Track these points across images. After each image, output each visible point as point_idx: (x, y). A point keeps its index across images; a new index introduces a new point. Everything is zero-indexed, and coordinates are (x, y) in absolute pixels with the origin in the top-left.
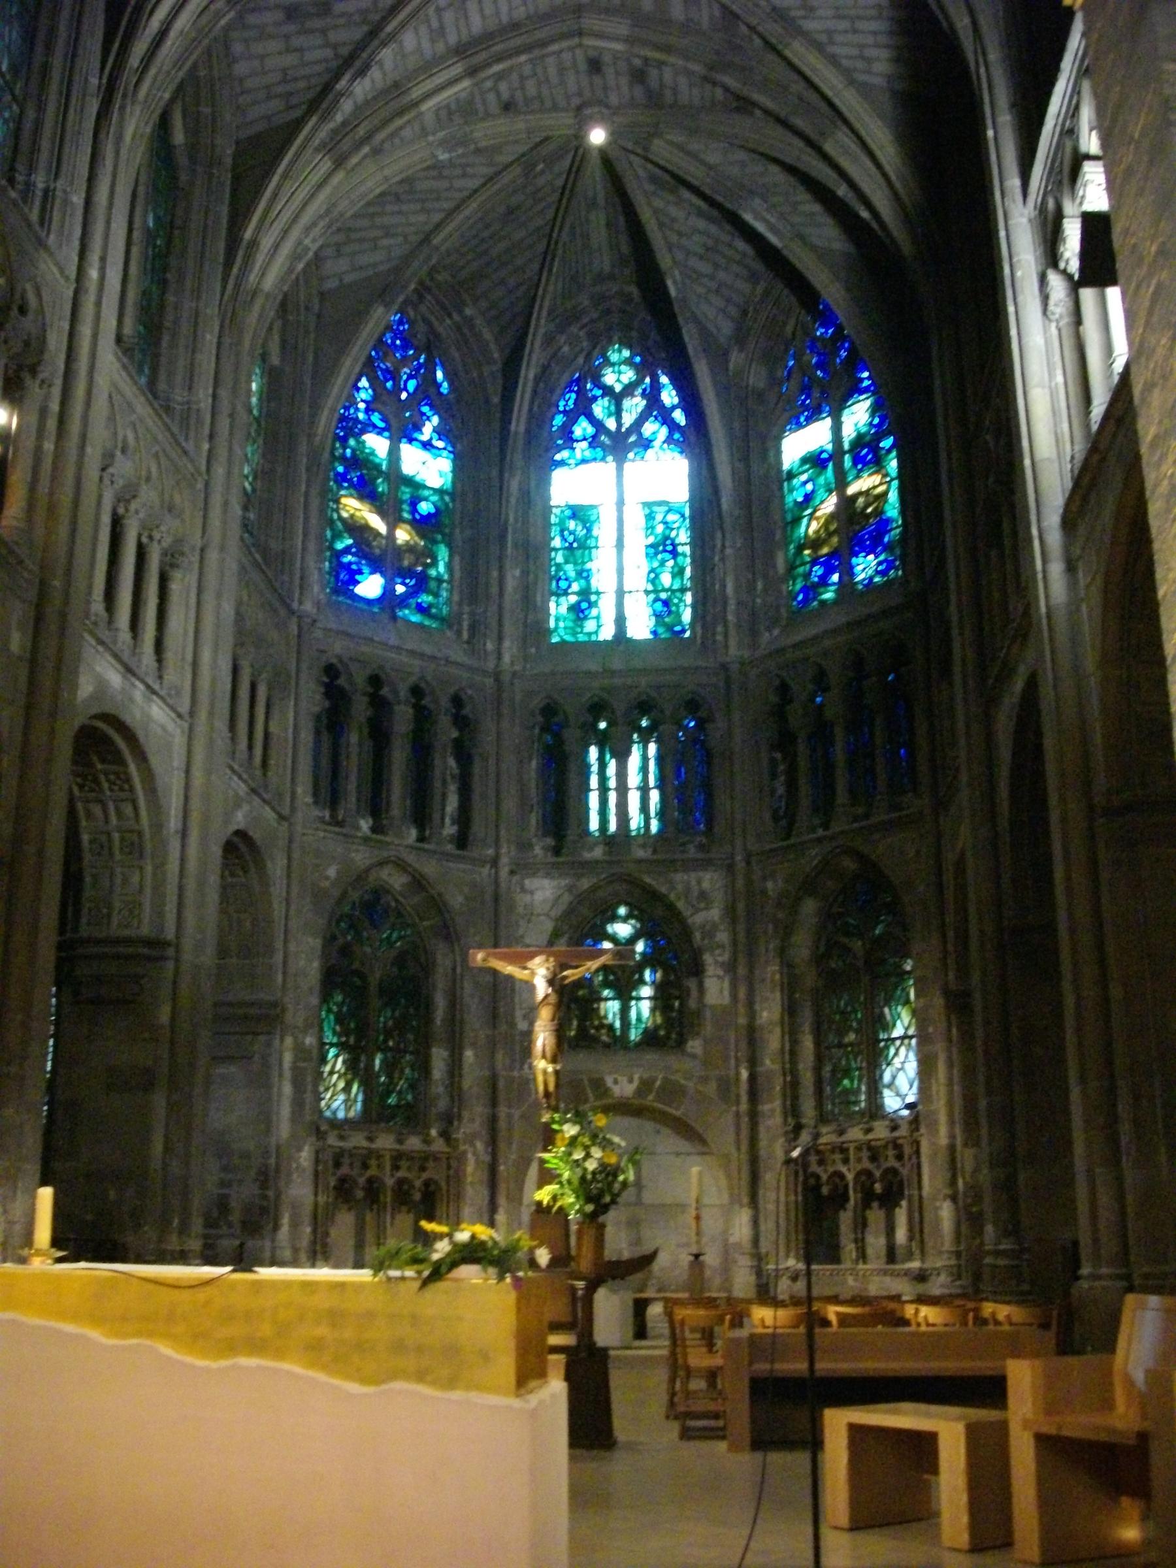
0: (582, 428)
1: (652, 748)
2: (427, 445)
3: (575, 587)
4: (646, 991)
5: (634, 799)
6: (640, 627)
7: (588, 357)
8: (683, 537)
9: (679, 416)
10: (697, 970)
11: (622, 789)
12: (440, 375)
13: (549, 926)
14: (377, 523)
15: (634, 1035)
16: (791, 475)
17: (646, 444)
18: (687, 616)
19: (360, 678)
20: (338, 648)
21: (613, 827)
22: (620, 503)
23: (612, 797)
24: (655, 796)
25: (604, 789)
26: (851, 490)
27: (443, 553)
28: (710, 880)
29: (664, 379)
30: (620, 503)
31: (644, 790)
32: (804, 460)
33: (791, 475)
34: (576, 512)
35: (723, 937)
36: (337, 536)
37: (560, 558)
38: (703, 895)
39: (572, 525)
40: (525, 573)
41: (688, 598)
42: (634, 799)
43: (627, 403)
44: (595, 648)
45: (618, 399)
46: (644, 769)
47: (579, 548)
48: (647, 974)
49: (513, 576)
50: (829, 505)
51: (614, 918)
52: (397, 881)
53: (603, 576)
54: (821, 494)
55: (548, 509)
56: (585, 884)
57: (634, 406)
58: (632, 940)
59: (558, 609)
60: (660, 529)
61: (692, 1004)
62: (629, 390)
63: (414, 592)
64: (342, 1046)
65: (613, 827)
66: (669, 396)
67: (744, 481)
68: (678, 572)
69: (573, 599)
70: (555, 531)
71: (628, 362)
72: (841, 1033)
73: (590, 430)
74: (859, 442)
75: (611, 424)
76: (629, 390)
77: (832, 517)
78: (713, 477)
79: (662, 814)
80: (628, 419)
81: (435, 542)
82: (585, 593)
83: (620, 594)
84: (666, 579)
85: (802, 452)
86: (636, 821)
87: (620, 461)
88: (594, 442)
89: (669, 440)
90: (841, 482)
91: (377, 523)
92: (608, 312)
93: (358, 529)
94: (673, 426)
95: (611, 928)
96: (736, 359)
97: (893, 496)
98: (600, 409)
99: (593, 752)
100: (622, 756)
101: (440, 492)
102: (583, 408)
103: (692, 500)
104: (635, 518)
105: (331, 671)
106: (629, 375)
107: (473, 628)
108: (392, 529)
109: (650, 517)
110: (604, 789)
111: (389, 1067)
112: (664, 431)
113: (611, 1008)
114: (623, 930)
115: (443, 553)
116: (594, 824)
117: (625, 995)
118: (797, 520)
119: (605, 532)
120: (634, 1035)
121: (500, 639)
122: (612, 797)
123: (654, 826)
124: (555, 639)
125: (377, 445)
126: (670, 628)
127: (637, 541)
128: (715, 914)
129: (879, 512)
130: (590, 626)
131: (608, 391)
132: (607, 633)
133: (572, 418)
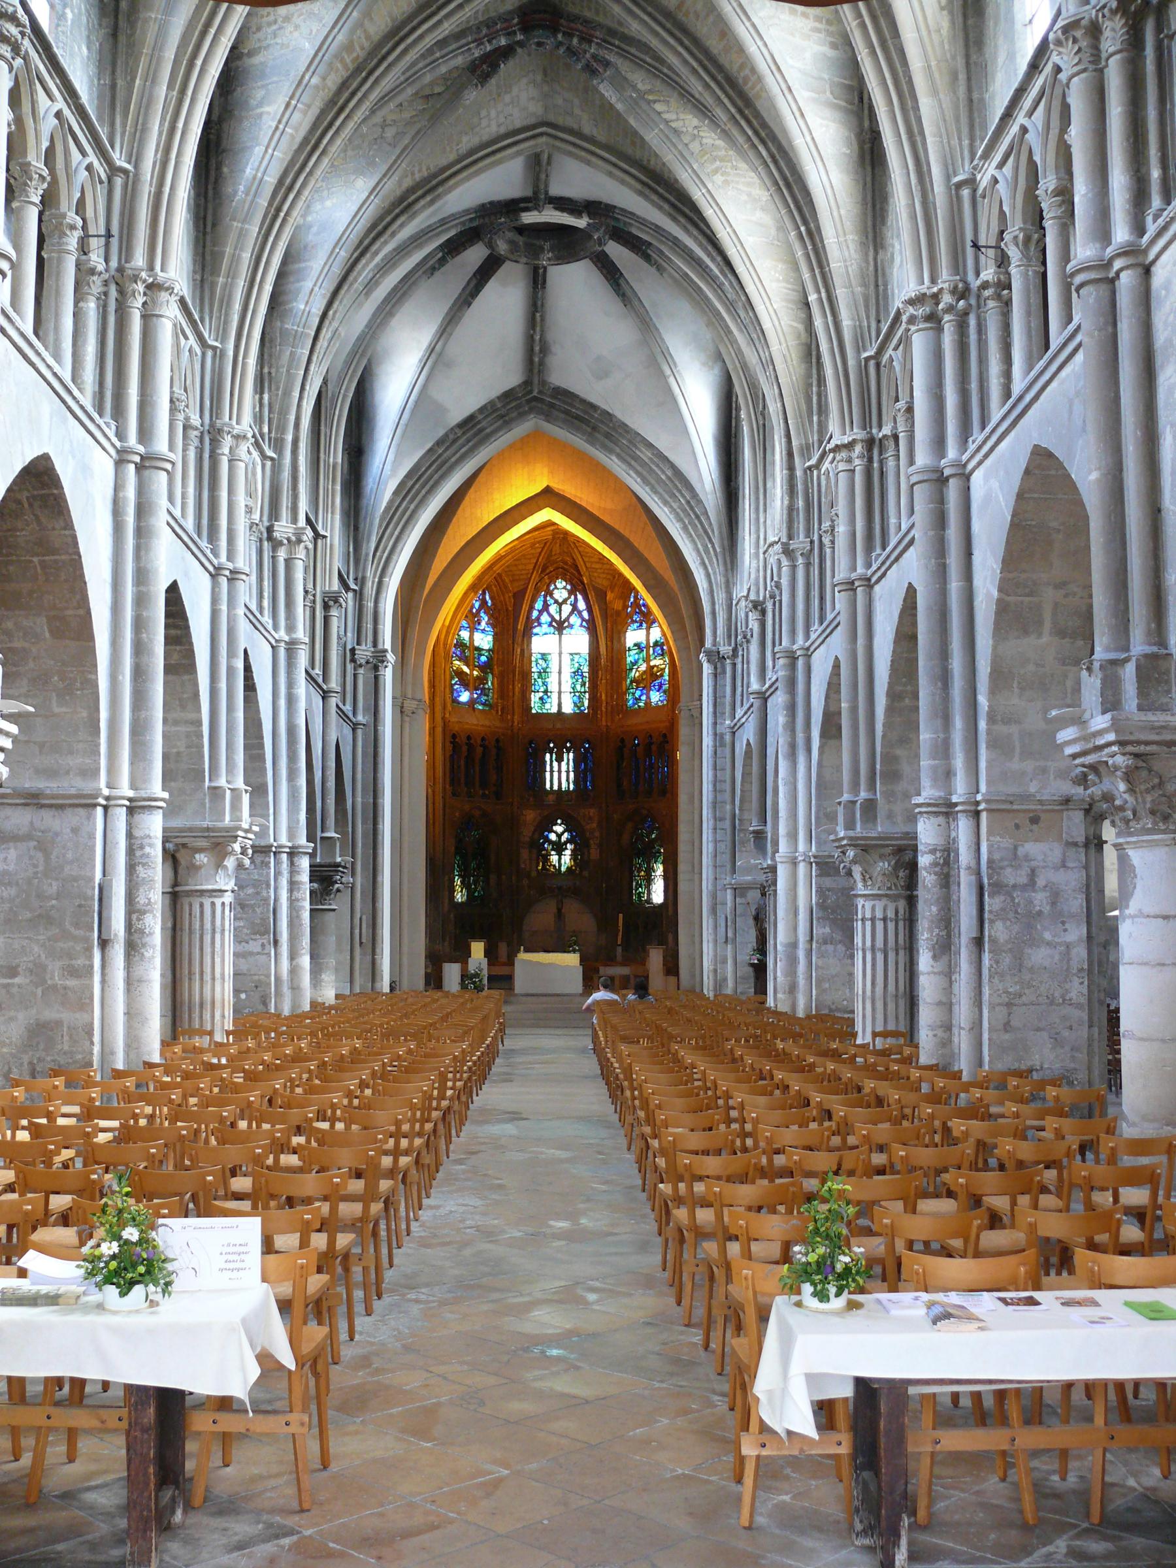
0: (545, 618)
1: (571, 755)
2: (483, 631)
3: (542, 689)
4: (568, 852)
5: (564, 775)
6: (568, 708)
7: (548, 586)
8: (586, 669)
9: (586, 615)
10: (588, 846)
11: (560, 772)
12: (487, 597)
13: (532, 829)
14: (466, 669)
15: (563, 869)
16: (630, 650)
17: (571, 626)
18: (586, 703)
19: (464, 740)
20: (456, 728)
21: (556, 787)
22: (560, 654)
23: (556, 775)
24: (572, 775)
25: (552, 771)
26: (652, 663)
27: (490, 677)
28: (592, 812)
29: (580, 597)
30: (560, 654)
31: (568, 772)
32: (635, 645)
33: (630, 650)
34: (544, 657)
35: (597, 834)
36: (452, 678)
37: (535, 676)
38: (590, 818)
39: (540, 662)
40: (522, 685)
41: (587, 695)
42: (564, 775)
43: (564, 607)
44: (548, 716)
45: (560, 605)
46: (568, 764)
47: (544, 672)
48: (569, 846)
49: (518, 686)
50: (643, 667)
51: (556, 824)
52: (477, 813)
53: (553, 686)
54: (641, 662)
55: (531, 655)
56: (546, 813)
57: (567, 609)
58: (563, 833)
59: (535, 698)
60: (576, 665)
61: (586, 858)
62: (565, 601)
63: (479, 696)
64: (460, 876)
65: (556, 787)
66: (582, 605)
67: (610, 649)
68: (583, 684)
69: (541, 694)
70: (533, 664)
71: (565, 588)
72: (639, 872)
73: (549, 619)
74: (656, 644)
75: (557, 617)
76: (565, 601)
77: (645, 672)
78: (598, 647)
79: (575, 782)
80: (564, 616)
81: (486, 673)
82: (546, 692)
83: (560, 693)
84: (578, 687)
85: (635, 641)
86: (564, 786)
87: (560, 634)
88: (550, 625)
89: (581, 626)
90: (647, 660)
91: (466, 669)
92: (557, 568)
93: (460, 674)
94: (583, 620)
95: (555, 828)
96: (610, 596)
97: (667, 670)
98: (553, 609)
99: (548, 756)
100: (560, 760)
101: (489, 651)
102: (546, 607)
103: (590, 654)
104: (566, 659)
105: (454, 736)
106: (565, 594)
107: (502, 709)
108: (472, 671)
109: (572, 660)
110: (552, 771)
111: (475, 883)
112: (579, 621)
113: (554, 858)
114: (559, 829)
115: (490, 677)
116: (548, 786)
117: (560, 855)
118: (631, 669)
119: (554, 667)
120: (563, 869)
121: (513, 714)
122: (556, 775)
123: (572, 787)
124: (534, 711)
125: (465, 635)
126: (579, 708)
127: (567, 671)
128: (595, 825)
129: (662, 675)
130: (547, 706)
131: (556, 602)
132: (554, 710)
133: (541, 612)
